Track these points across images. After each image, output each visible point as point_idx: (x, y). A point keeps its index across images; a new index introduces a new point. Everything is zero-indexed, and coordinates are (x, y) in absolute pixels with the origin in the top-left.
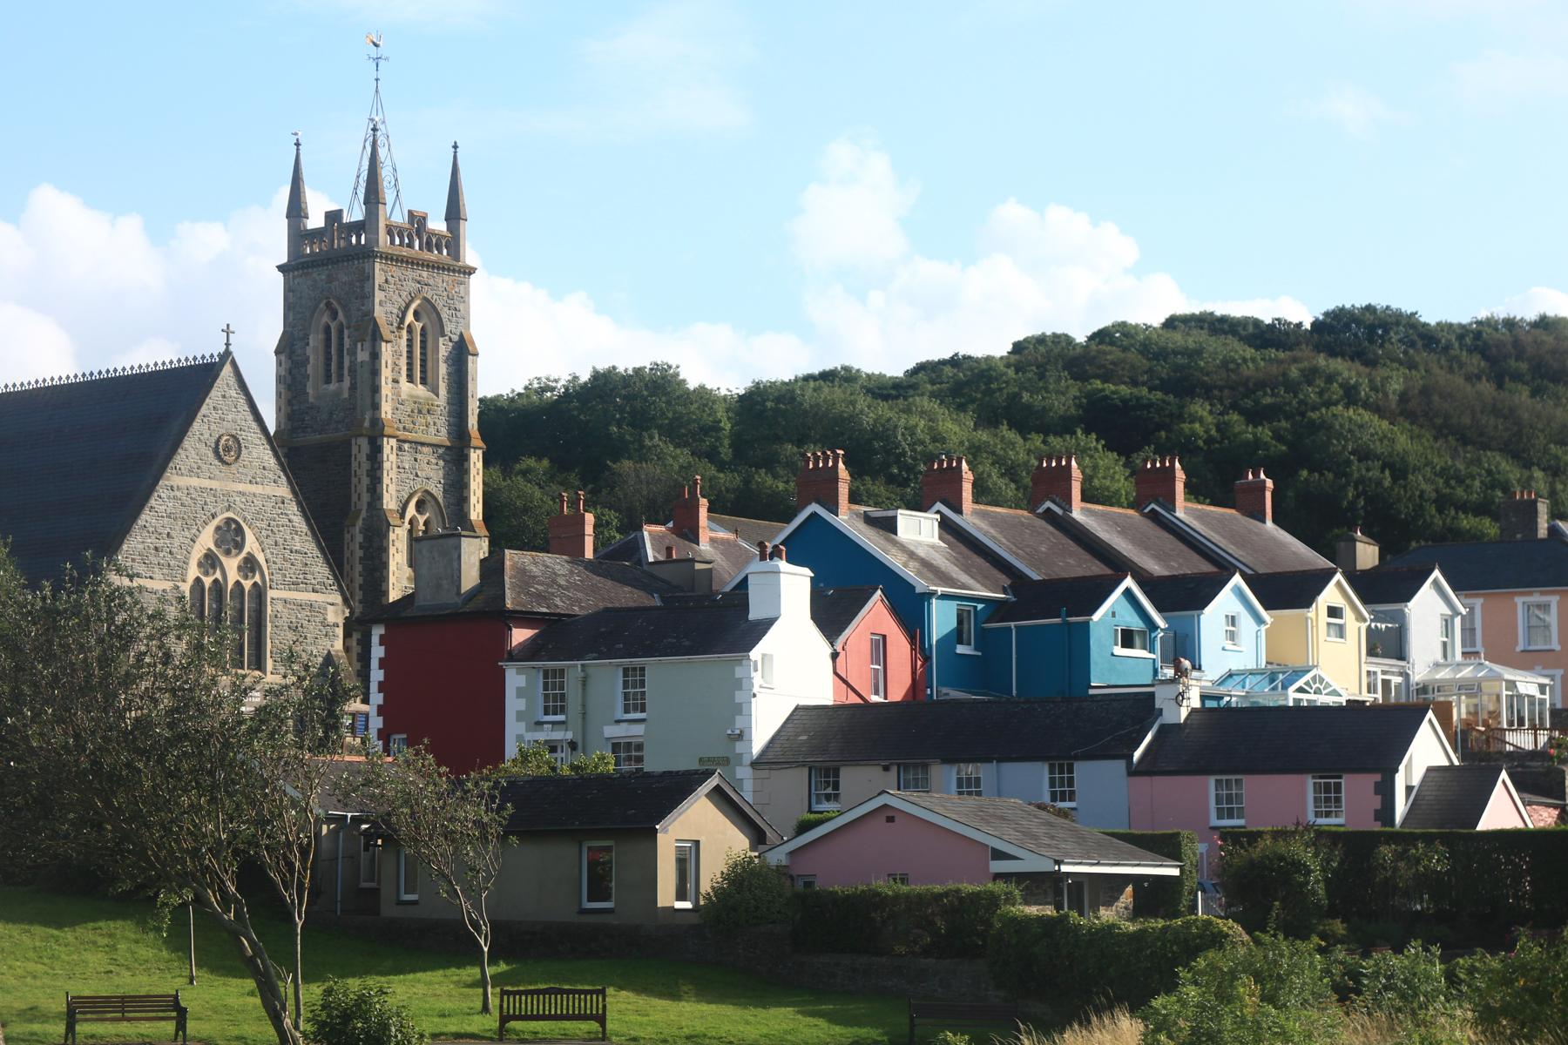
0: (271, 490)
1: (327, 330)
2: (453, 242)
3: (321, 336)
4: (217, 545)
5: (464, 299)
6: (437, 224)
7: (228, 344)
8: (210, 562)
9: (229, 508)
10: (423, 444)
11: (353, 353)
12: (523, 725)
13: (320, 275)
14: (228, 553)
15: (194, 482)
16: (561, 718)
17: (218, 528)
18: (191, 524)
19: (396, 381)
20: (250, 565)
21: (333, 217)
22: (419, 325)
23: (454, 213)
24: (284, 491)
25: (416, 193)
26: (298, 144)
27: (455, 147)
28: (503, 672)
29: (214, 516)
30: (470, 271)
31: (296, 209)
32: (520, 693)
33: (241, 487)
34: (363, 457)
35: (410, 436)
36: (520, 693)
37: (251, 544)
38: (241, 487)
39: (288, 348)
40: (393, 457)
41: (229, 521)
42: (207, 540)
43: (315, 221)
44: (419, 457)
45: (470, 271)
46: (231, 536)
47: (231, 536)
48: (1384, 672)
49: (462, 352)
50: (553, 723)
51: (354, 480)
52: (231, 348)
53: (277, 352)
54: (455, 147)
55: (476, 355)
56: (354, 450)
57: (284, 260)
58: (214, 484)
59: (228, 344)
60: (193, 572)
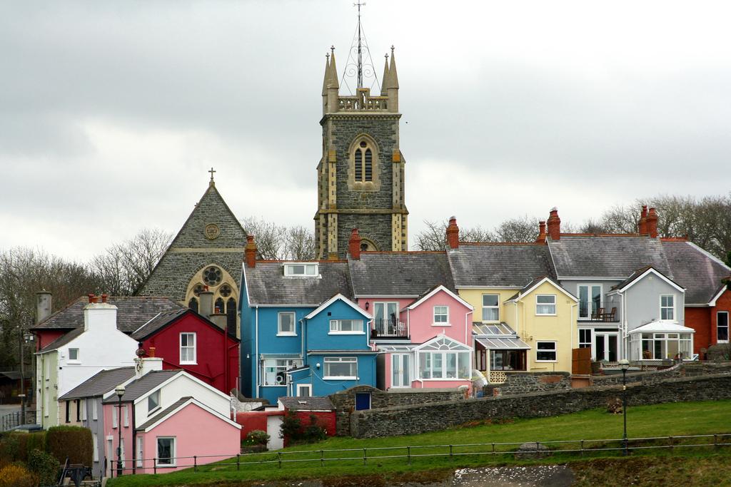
4: (206, 280)
7: (212, 178)
8: (199, 290)
9: (213, 262)
15: (190, 250)
17: (206, 272)
20: (226, 290)
22: (363, 150)
30: (399, 117)
33: (220, 250)
37: (226, 277)
38: (220, 250)
40: (336, 224)
41: (213, 269)
42: (199, 278)
46: (212, 276)
47: (212, 276)
48: (596, 330)
58: (202, 250)
59: (212, 178)
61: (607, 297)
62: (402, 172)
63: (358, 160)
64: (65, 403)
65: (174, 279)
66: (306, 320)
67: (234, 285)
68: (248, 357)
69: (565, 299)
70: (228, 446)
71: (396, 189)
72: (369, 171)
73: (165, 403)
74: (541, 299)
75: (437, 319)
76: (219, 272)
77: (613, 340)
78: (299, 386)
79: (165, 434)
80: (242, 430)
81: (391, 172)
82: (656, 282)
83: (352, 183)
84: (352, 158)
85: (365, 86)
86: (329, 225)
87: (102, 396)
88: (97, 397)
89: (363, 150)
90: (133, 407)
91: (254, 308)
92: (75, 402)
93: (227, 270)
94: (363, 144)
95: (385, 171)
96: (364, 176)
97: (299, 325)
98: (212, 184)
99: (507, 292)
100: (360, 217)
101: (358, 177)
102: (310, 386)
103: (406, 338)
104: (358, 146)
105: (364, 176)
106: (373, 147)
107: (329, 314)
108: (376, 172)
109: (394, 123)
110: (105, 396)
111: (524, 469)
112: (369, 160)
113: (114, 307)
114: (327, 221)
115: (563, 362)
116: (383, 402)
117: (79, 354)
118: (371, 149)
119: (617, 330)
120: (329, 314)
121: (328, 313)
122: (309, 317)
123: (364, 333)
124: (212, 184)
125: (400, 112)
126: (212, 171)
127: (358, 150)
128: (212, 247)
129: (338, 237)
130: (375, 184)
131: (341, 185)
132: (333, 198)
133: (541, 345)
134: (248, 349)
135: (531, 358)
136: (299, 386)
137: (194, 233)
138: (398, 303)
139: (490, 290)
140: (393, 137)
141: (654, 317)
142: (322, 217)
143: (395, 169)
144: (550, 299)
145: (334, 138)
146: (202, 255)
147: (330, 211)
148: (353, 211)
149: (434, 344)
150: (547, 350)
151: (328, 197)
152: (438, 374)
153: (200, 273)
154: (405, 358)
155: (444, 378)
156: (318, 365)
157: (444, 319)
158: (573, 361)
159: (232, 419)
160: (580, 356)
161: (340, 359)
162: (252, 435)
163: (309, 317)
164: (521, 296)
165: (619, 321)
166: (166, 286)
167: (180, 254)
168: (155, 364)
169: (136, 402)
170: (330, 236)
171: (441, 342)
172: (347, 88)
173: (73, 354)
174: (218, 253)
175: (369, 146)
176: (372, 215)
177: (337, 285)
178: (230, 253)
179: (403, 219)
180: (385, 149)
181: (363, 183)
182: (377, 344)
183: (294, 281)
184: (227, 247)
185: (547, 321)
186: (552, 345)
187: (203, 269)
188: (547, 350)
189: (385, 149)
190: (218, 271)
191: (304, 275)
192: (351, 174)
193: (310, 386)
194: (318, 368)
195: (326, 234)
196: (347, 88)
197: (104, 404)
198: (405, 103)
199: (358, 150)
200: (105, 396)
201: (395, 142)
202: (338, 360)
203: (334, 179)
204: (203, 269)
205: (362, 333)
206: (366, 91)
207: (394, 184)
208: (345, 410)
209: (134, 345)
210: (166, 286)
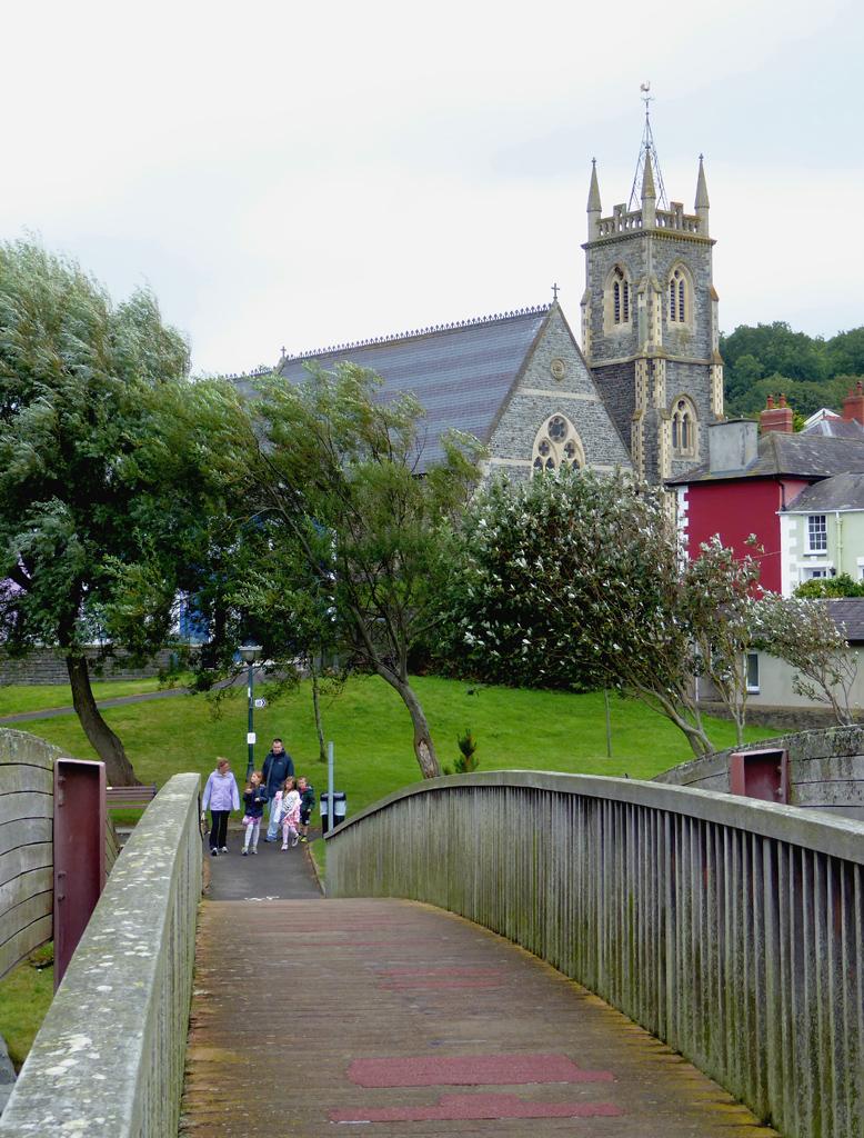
0: (585, 396)
1: (617, 285)
2: (696, 222)
3: (612, 292)
4: (550, 435)
5: (708, 263)
6: (689, 210)
7: (556, 298)
10: (682, 363)
11: (635, 302)
12: (795, 557)
13: (612, 250)
14: (556, 440)
15: (537, 392)
16: (822, 551)
17: (551, 423)
18: (533, 418)
19: (664, 320)
20: (570, 450)
21: (618, 209)
23: (702, 203)
24: (593, 397)
25: (677, 190)
26: (594, 162)
27: (701, 157)
28: (778, 517)
29: (549, 415)
30: (712, 243)
31: (594, 205)
32: (793, 533)
33: (566, 395)
34: (643, 373)
35: (673, 357)
36: (793, 533)
37: (572, 433)
38: (566, 395)
39: (591, 302)
40: (664, 372)
41: (557, 419)
42: (544, 432)
43: (607, 212)
44: (680, 371)
45: (712, 243)
46: (557, 430)
47: (557, 430)
49: (709, 297)
50: (818, 555)
51: (637, 389)
52: (558, 300)
53: (582, 304)
54: (701, 157)
55: (717, 300)
56: (637, 368)
57: (586, 241)
58: (548, 393)
59: (556, 298)
60: (536, 453)
65: (521, 430)
67: (579, 443)
89: (678, 282)
93: (573, 423)
95: (701, 311)
96: (678, 315)
100: (681, 366)
105: (678, 315)
106: (687, 278)
125: (712, 236)
126: (555, 289)
128: (559, 389)
130: (691, 326)
137: (540, 368)
140: (707, 268)
151: (651, 339)
153: (546, 423)
175: (682, 277)
176: (691, 365)
181: (678, 324)
187: (549, 419)
189: (701, 282)
190: (562, 425)
201: (709, 275)
210: (513, 439)
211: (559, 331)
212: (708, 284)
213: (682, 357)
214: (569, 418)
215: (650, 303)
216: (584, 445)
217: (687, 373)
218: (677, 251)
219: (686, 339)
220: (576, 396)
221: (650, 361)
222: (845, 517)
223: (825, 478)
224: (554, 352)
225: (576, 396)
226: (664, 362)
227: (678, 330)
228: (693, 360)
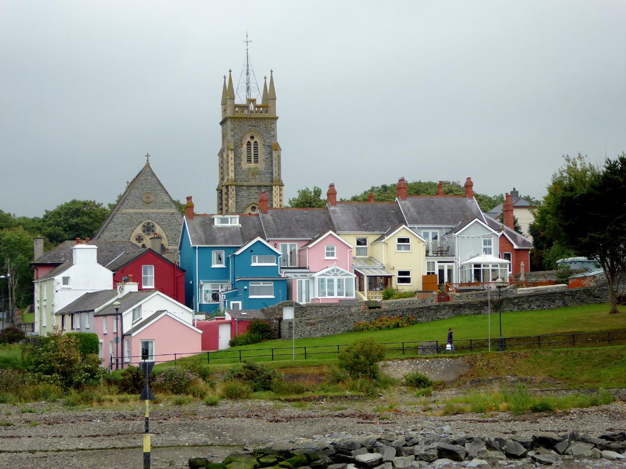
0: (167, 210)
4: (144, 231)
5: (274, 130)
7: (148, 161)
9: (149, 218)
17: (144, 226)
18: (132, 225)
22: (252, 142)
27: (272, 72)
29: (141, 222)
30: (276, 118)
33: (154, 211)
38: (154, 211)
40: (234, 193)
41: (149, 224)
42: (139, 230)
47: (148, 229)
48: (439, 262)
54: (272, 72)
58: (141, 211)
59: (148, 161)
61: (442, 239)
62: (279, 156)
63: (249, 149)
64: (61, 316)
65: (122, 231)
66: (234, 256)
68: (191, 283)
69: (417, 240)
70: (192, 347)
71: (275, 169)
72: (256, 156)
73: (145, 316)
74: (401, 240)
75: (328, 254)
76: (153, 226)
77: (450, 272)
78: (232, 303)
79: (146, 338)
80: (203, 335)
81: (272, 157)
82: (479, 227)
83: (245, 165)
84: (245, 147)
85: (253, 97)
86: (229, 193)
87: (93, 311)
88: (88, 311)
89: (252, 142)
90: (122, 317)
91: (195, 248)
92: (69, 315)
93: (159, 224)
94: (252, 137)
95: (267, 157)
97: (227, 259)
98: (148, 165)
99: (375, 236)
100: (251, 188)
101: (249, 161)
102: (240, 303)
103: (305, 268)
104: (249, 139)
106: (259, 140)
107: (252, 251)
108: (261, 157)
109: (274, 123)
110: (96, 310)
111: (428, 361)
112: (256, 148)
113: (95, 246)
114: (228, 191)
115: (416, 283)
116: (303, 313)
117: (71, 281)
118: (258, 141)
119: (453, 262)
120: (252, 251)
121: (251, 250)
122: (238, 253)
123: (277, 265)
124: (148, 165)
125: (277, 115)
126: (148, 156)
127: (249, 142)
129: (236, 202)
130: (261, 166)
131: (237, 165)
132: (232, 175)
133: (400, 273)
134: (192, 277)
135: (395, 280)
136: (232, 303)
138: (297, 244)
139: (362, 235)
140: (273, 133)
141: (478, 251)
142: (224, 190)
143: (275, 154)
144: (406, 240)
145: (232, 133)
146: (141, 214)
147: (229, 183)
148: (246, 184)
149: (328, 272)
150: (404, 276)
151: (228, 175)
152: (331, 294)
153: (140, 226)
154: (308, 283)
155: (336, 296)
156: (246, 287)
157: (333, 254)
158: (423, 284)
159: (194, 325)
160: (428, 279)
161: (261, 283)
162: (209, 337)
163: (238, 253)
164: (386, 238)
165: (454, 256)
166: (116, 236)
167: (125, 214)
168: (131, 287)
169: (123, 314)
170: (231, 201)
171: (333, 270)
172: (240, 99)
173: (66, 280)
174: (152, 213)
175: (256, 139)
177: (254, 232)
178: (161, 213)
179: (281, 190)
180: (268, 141)
182: (285, 273)
183: (221, 229)
184: (158, 209)
185: (405, 256)
186: (407, 273)
187: (142, 224)
188: (404, 276)
189: (268, 141)
191: (229, 225)
192: (244, 158)
193: (240, 303)
194: (246, 290)
195: (227, 200)
196: (240, 99)
197: (95, 316)
198: (281, 109)
199: (249, 142)
200: (96, 310)
201: (274, 136)
202: (260, 284)
203: (233, 161)
204: (142, 224)
205: (274, 264)
206: (254, 101)
207: (274, 165)
208: (276, 319)
209: (109, 274)
210: (116, 236)
211: (150, 178)
212: (273, 141)
213: (253, 183)
214: (157, 223)
215: (228, 156)
216: (167, 236)
217: (256, 191)
218: (250, 126)
219: (255, 173)
220: (162, 211)
221: (227, 187)
222: (43, 283)
223: (61, 264)
224: (145, 189)
225: (162, 211)
226: (234, 187)
227: (250, 169)
228: (260, 184)
